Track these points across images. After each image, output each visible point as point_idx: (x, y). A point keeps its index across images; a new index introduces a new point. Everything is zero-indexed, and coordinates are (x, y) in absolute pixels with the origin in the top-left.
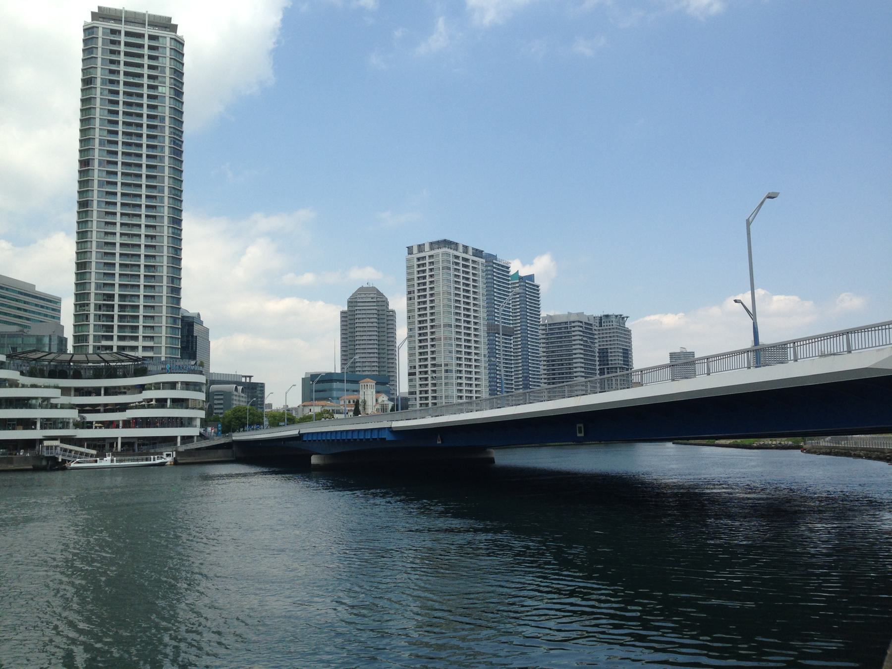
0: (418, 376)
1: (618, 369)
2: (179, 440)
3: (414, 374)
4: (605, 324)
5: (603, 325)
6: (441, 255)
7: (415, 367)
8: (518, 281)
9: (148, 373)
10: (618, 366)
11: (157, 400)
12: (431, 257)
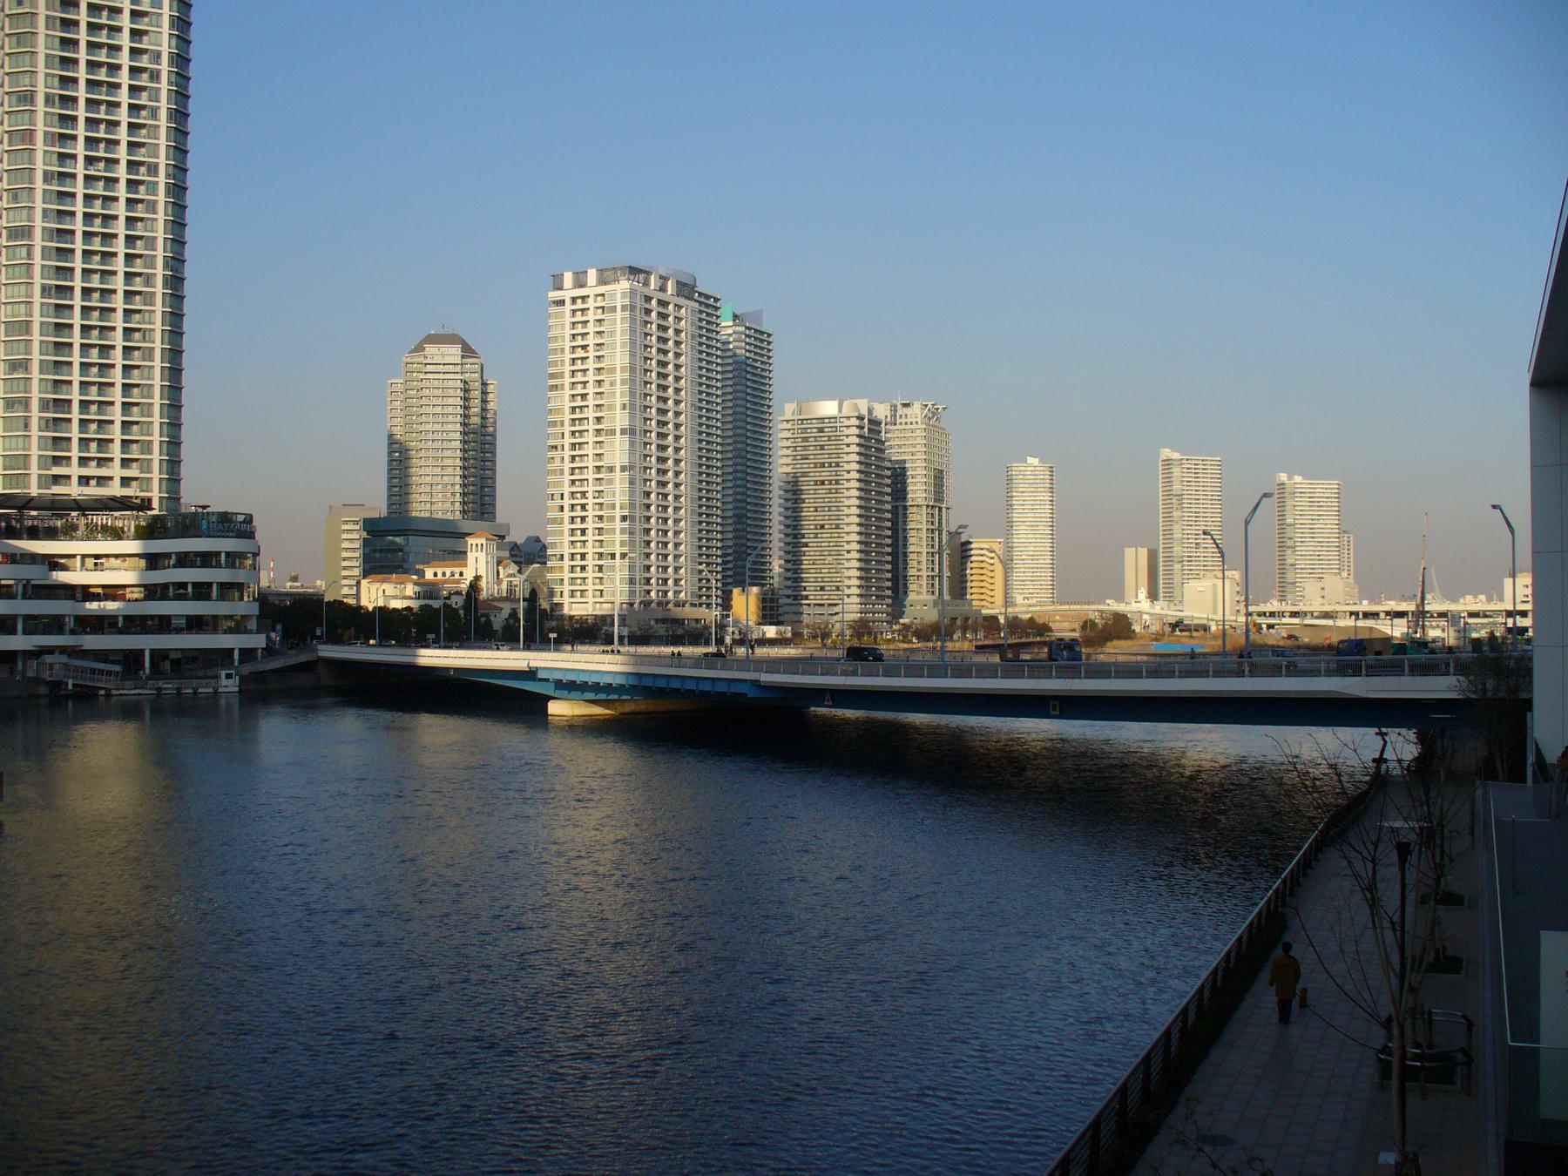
2: (236, 655)
4: (903, 420)
5: (898, 421)
8: (731, 323)
11: (196, 585)
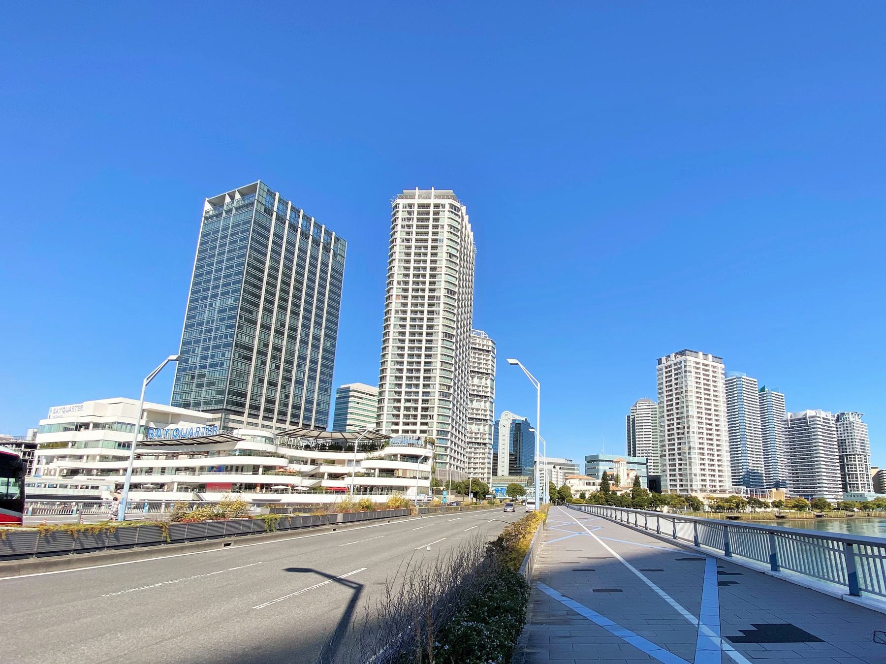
1: (856, 456)
3: (665, 456)
10: (856, 453)
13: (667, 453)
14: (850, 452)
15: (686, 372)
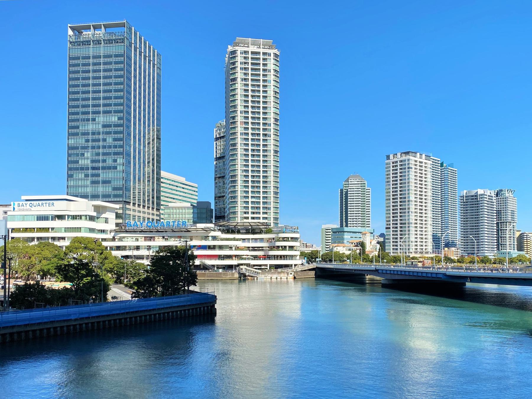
0: (392, 229)
1: (508, 223)
3: (389, 228)
6: (407, 160)
7: (390, 225)
9: (273, 232)
10: (507, 221)
12: (401, 161)
13: (391, 226)
14: (503, 220)
15: (409, 168)
